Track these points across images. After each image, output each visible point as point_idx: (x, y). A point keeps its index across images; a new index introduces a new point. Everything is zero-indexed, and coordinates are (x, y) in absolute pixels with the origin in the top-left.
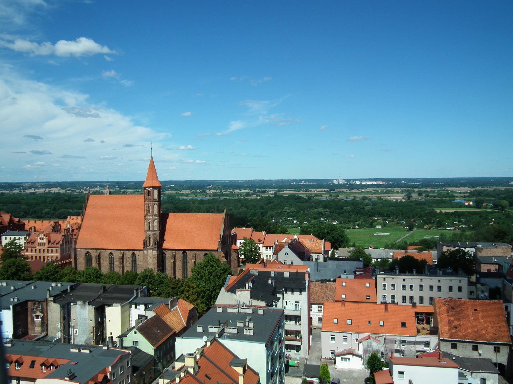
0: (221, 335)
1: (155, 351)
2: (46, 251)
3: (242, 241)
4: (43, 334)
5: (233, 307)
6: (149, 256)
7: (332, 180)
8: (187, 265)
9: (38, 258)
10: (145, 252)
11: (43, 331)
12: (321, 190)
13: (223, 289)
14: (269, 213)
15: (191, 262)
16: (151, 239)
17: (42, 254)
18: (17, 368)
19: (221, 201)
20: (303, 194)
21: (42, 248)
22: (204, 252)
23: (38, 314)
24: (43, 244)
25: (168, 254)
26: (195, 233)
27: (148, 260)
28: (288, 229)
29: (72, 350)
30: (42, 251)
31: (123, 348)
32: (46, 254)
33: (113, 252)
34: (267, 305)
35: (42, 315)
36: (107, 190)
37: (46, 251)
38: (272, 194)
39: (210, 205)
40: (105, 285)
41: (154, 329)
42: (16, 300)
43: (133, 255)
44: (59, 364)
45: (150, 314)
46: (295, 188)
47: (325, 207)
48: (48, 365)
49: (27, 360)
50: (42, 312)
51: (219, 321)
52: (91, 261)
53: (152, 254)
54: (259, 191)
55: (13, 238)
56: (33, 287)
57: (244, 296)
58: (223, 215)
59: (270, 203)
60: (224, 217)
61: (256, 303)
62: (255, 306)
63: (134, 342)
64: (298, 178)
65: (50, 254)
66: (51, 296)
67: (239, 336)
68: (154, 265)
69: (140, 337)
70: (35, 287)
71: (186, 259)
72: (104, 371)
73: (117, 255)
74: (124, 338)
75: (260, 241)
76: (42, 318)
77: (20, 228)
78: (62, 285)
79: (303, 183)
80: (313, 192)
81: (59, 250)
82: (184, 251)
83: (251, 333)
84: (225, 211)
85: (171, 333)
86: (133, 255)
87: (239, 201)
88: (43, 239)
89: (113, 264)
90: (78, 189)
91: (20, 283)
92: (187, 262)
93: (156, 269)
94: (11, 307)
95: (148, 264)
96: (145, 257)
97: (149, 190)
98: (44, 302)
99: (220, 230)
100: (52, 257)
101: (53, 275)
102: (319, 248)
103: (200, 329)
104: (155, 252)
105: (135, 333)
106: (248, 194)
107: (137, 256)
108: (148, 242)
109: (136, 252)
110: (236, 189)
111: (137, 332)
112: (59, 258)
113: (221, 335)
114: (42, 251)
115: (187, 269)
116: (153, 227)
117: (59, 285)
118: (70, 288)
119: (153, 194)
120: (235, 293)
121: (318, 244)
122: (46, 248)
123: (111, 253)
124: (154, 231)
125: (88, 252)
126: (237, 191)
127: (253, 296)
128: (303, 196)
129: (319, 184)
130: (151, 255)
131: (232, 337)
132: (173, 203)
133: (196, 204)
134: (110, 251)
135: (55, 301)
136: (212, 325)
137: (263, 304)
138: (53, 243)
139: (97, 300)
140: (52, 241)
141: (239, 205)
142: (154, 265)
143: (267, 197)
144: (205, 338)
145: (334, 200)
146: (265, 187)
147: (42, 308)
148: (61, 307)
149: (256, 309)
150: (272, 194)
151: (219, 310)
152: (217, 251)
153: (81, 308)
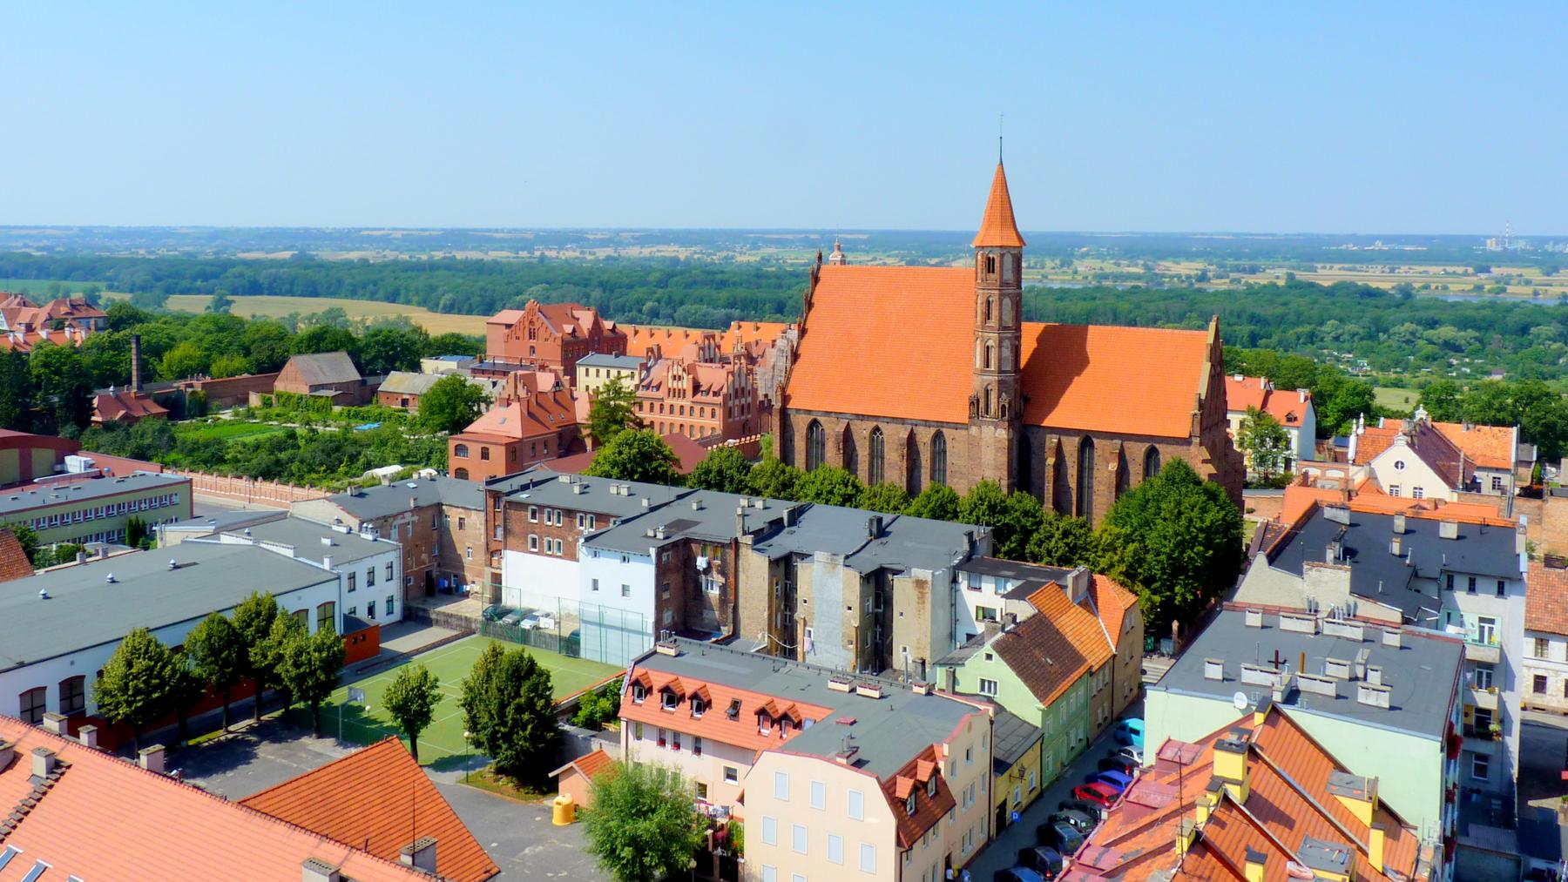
0: (1292, 696)
2: (687, 411)
3: (1241, 417)
5: (1295, 613)
6: (983, 443)
7: (1479, 240)
9: (676, 430)
10: (974, 430)
12: (1439, 269)
13: (1260, 561)
15: (1105, 470)
17: (677, 419)
18: (697, 715)
20: (1379, 279)
21: (677, 402)
24: (681, 393)
27: (981, 458)
28: (1376, 390)
29: (831, 685)
30: (677, 409)
31: (955, 693)
32: (686, 420)
34: (1406, 621)
35: (722, 580)
36: (836, 252)
37: (687, 411)
40: (879, 514)
41: (1037, 652)
43: (938, 436)
44: (803, 717)
46: (1358, 261)
47: (1463, 324)
48: (776, 716)
49: (721, 698)
50: (723, 572)
54: (1237, 269)
56: (695, 506)
57: (1329, 583)
61: (1367, 609)
62: (1366, 620)
63: (983, 681)
64: (1363, 230)
65: (696, 420)
66: (745, 533)
67: (1342, 703)
68: (997, 468)
69: (1001, 671)
71: (1091, 458)
72: (930, 754)
74: (959, 670)
75: (1291, 419)
76: (723, 588)
77: (615, 345)
79: (1378, 245)
80: (1412, 275)
81: (719, 412)
82: (1087, 441)
84: (1212, 325)
85: (1082, 669)
86: (938, 436)
92: (1091, 469)
93: (1005, 482)
94: (653, 551)
96: (974, 444)
102: (1499, 454)
103: (1214, 672)
104: (1003, 434)
105: (989, 657)
106: (1203, 277)
107: (948, 441)
108: (982, 404)
111: (995, 655)
112: (719, 432)
113: (1292, 696)
114: (677, 409)
115: (1091, 488)
116: (1000, 360)
120: (1300, 573)
121: (1495, 442)
122: (687, 403)
123: (877, 429)
127: (1360, 588)
128: (1385, 286)
129: (1437, 251)
137: (1395, 615)
142: (997, 468)
144: (1241, 700)
145: (1492, 305)
146: (1253, 257)
147: (724, 561)
148: (770, 562)
151: (1254, 620)
152: (1186, 442)
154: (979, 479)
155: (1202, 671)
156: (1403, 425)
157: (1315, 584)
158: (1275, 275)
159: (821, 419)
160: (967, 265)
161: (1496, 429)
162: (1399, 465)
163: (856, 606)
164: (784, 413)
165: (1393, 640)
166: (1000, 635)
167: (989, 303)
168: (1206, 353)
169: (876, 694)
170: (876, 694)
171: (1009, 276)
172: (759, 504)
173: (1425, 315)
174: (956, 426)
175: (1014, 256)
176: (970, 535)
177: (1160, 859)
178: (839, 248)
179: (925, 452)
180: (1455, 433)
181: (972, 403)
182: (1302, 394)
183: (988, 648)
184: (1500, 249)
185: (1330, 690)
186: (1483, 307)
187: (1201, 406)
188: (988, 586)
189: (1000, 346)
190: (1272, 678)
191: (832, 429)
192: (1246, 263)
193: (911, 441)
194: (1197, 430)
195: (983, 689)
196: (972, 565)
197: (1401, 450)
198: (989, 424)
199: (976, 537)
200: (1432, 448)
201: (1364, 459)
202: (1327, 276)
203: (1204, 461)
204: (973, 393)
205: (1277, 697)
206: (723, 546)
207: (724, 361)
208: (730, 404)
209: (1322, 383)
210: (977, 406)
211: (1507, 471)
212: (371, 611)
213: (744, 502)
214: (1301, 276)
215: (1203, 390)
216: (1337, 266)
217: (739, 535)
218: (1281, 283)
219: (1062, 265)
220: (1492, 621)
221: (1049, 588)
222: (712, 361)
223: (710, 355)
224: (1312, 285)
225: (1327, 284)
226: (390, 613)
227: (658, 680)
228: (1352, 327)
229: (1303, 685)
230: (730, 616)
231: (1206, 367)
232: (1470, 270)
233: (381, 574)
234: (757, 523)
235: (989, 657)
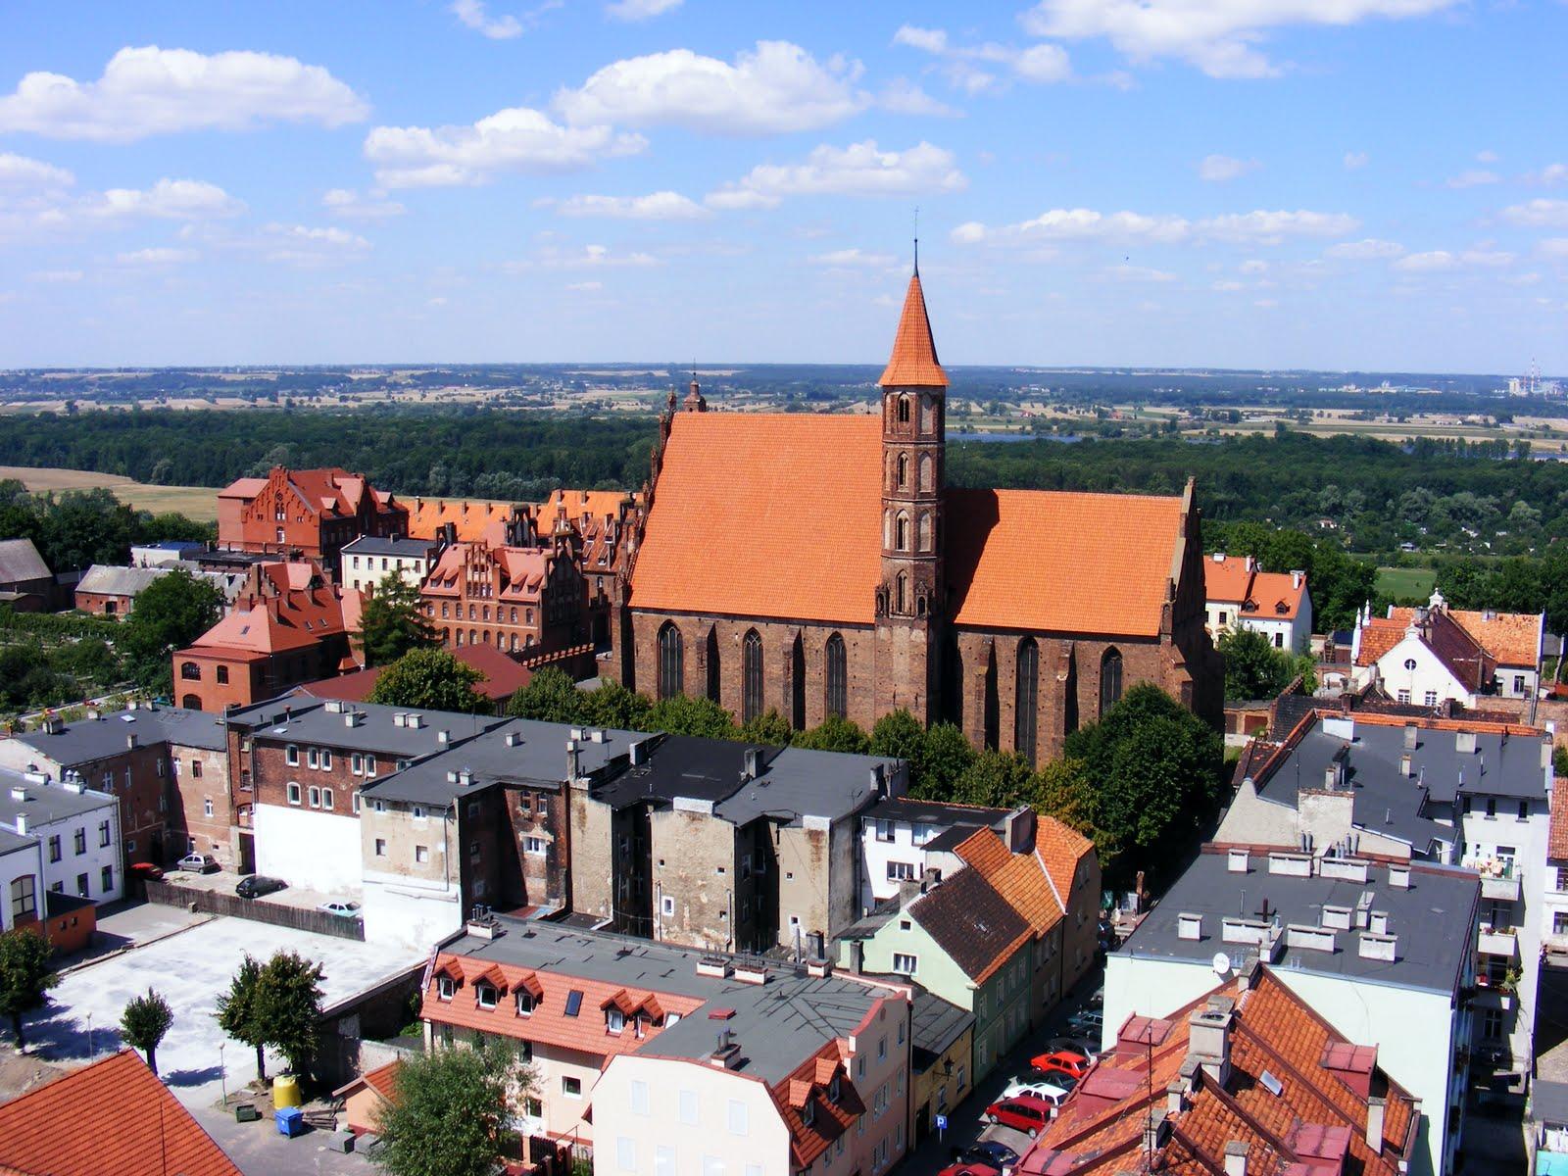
0: (1280, 954)
1: (977, 994)
4: (554, 906)
6: (895, 649)
7: (1501, 381)
8: (1034, 689)
10: (883, 632)
11: (552, 893)
15: (1052, 681)
16: (908, 586)
20: (1386, 429)
22: (1106, 645)
23: (538, 832)
25: (966, 643)
26: (1080, 569)
27: (893, 668)
29: (702, 969)
33: (760, 627)
34: (1415, 855)
35: (549, 837)
42: (465, 781)
43: (835, 641)
44: (665, 1010)
45: (949, 864)
47: (1482, 488)
48: (628, 1010)
49: (555, 989)
50: (550, 826)
51: (1266, 903)
52: (681, 657)
53: (908, 641)
55: (392, 562)
56: (509, 741)
57: (1327, 815)
58: (1184, 503)
60: (1185, 509)
62: (1370, 857)
64: (1367, 367)
66: (578, 775)
67: (1343, 960)
68: (912, 682)
69: (921, 943)
70: (517, 743)
71: (1035, 665)
72: (831, 1051)
73: (776, 641)
74: (866, 943)
76: (552, 849)
78: (605, 741)
79: (1385, 388)
82: (1028, 639)
83: (1388, 953)
85: (1024, 937)
86: (835, 643)
88: (483, 569)
89: (761, 672)
91: (467, 724)
92: (1035, 680)
93: (923, 700)
95: (891, 678)
96: (882, 651)
97: (904, 397)
98: (558, 792)
99: (1167, 561)
100: (514, 636)
102: (1523, 647)
103: (1190, 930)
104: (920, 636)
107: (849, 646)
108: (893, 597)
109: (844, 632)
111: (914, 924)
113: (1280, 954)
115: (1034, 703)
116: (918, 540)
117: (597, 737)
118: (638, 748)
120: (1293, 802)
121: (1518, 634)
123: (752, 632)
125: (669, 624)
126: (1122, 411)
128: (1396, 439)
130: (906, 646)
131: (1314, 962)
134: (750, 624)
135: (595, 794)
136: (1242, 915)
137: (1401, 848)
138: (518, 587)
140: (514, 578)
142: (912, 682)
144: (1221, 962)
147: (552, 814)
148: (616, 817)
149: (1380, 864)
151: (1238, 863)
152: (1154, 640)
154: (889, 696)
155: (1175, 930)
156: (1416, 615)
157: (1311, 816)
158: (1261, 422)
159: (676, 619)
161: (1519, 617)
162: (1410, 664)
163: (730, 866)
164: (626, 612)
165: (1399, 879)
166: (920, 896)
167: (902, 462)
169: (760, 978)
170: (760, 978)
172: (597, 737)
173: (1443, 474)
174: (859, 626)
176: (879, 771)
177: (1125, 1159)
180: (1477, 624)
181: (880, 597)
182: (1296, 576)
183: (904, 914)
184: (1524, 393)
185: (1327, 944)
188: (903, 834)
189: (918, 520)
190: (1262, 934)
191: (692, 633)
192: (1225, 410)
194: (1169, 626)
195: (897, 966)
196: (879, 810)
197: (1413, 646)
198: (905, 622)
199: (886, 773)
200: (1449, 644)
201: (1370, 658)
202: (1328, 422)
203: (1178, 665)
205: (1265, 956)
206: (550, 792)
207: (543, 542)
209: (1321, 567)
211: (1531, 668)
212: (83, 880)
213: (576, 734)
215: (1175, 573)
216: (1336, 412)
217: (571, 779)
218: (1270, 434)
219: (993, 410)
220: (1512, 851)
221: (983, 834)
222: (525, 544)
223: (522, 533)
226: (107, 887)
227: (472, 969)
229: (1295, 940)
230: (563, 884)
231: (1181, 543)
232: (1492, 420)
233: (94, 838)
234: (595, 761)
235: (906, 925)
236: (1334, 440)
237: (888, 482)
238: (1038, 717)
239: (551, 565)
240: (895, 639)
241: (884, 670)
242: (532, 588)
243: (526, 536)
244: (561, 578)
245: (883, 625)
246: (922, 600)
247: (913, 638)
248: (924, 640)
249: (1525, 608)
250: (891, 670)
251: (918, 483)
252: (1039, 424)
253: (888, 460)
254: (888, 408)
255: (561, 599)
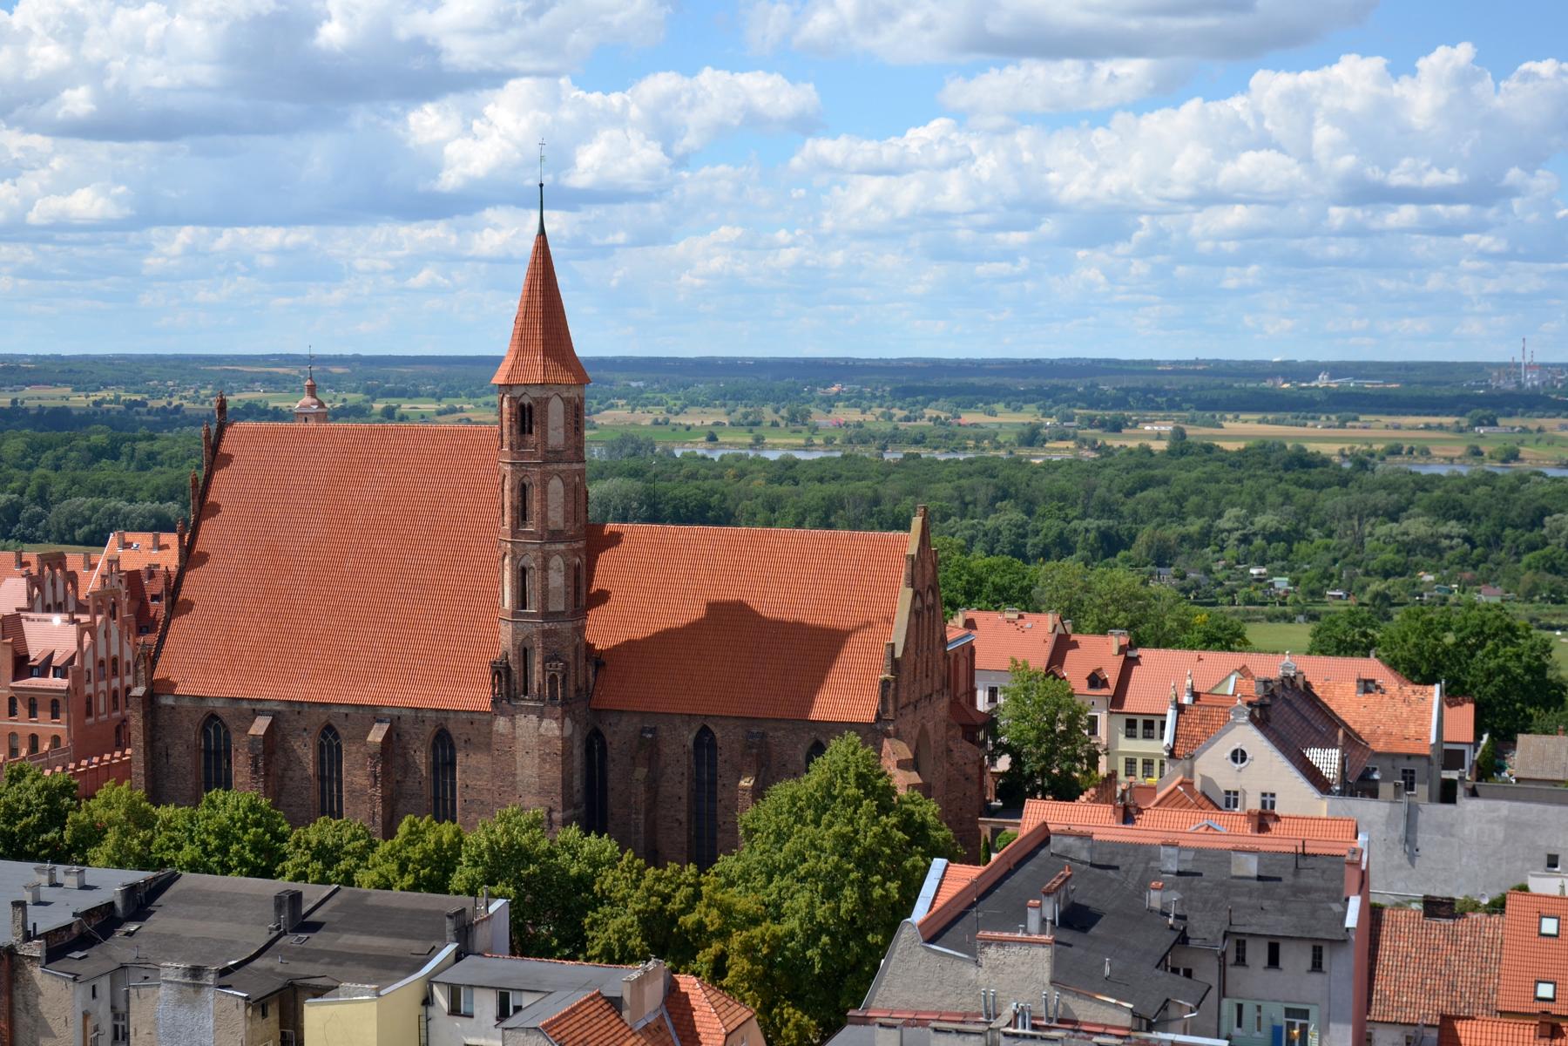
6: (518, 746)
14: (1145, 535)
19: (887, 471)
38: (1159, 437)
39: (831, 488)
54: (1091, 422)
58: (911, 541)
59: (1145, 485)
60: (913, 549)
66: (28, 937)
68: (543, 791)
71: (713, 764)
84: (917, 522)
87: (988, 470)
90: (154, 393)
95: (513, 786)
101: (42, 827)
106: (1032, 438)
110: (970, 406)
119: (544, 424)
124: (547, 615)
132: (635, 473)
133: (758, 484)
139: (258, 963)
141: (984, 493)
142: (543, 791)
143: (1131, 452)
146: (1120, 402)
150: (1159, 437)
153: (179, 1003)
160: (487, 416)
168: (904, 572)
171: (556, 436)
175: (567, 401)
178: (312, 390)
179: (424, 763)
186: (1476, 483)
187: (896, 665)
193: (392, 748)
198: (532, 710)
204: (497, 657)
208: (89, 689)
210: (509, 683)
214: (1194, 433)
218: (1159, 446)
224: (1209, 449)
225: (1231, 446)
228: (1267, 520)
231: (905, 595)
234: (58, 915)
236: (1240, 452)
237: (507, 519)
238: (719, 836)
239: (87, 637)
240: (519, 732)
241: (506, 778)
242: (61, 672)
243: (60, 598)
244: (102, 654)
245: (502, 714)
246: (553, 678)
247: (542, 730)
248: (557, 733)
249: (1429, 680)
250: (514, 775)
251: (544, 518)
252: (861, 436)
253: (507, 487)
254: (506, 416)
255: (103, 685)
